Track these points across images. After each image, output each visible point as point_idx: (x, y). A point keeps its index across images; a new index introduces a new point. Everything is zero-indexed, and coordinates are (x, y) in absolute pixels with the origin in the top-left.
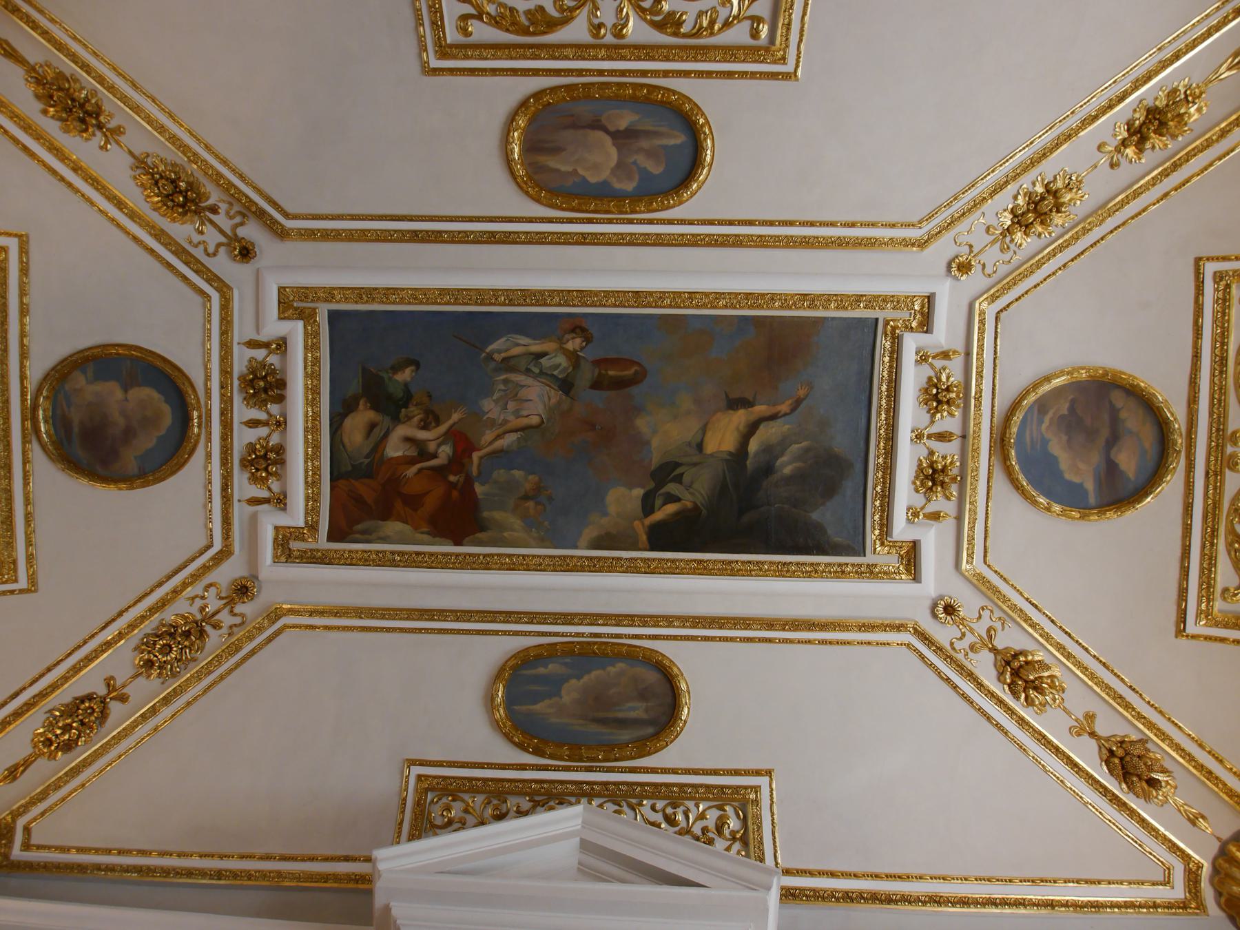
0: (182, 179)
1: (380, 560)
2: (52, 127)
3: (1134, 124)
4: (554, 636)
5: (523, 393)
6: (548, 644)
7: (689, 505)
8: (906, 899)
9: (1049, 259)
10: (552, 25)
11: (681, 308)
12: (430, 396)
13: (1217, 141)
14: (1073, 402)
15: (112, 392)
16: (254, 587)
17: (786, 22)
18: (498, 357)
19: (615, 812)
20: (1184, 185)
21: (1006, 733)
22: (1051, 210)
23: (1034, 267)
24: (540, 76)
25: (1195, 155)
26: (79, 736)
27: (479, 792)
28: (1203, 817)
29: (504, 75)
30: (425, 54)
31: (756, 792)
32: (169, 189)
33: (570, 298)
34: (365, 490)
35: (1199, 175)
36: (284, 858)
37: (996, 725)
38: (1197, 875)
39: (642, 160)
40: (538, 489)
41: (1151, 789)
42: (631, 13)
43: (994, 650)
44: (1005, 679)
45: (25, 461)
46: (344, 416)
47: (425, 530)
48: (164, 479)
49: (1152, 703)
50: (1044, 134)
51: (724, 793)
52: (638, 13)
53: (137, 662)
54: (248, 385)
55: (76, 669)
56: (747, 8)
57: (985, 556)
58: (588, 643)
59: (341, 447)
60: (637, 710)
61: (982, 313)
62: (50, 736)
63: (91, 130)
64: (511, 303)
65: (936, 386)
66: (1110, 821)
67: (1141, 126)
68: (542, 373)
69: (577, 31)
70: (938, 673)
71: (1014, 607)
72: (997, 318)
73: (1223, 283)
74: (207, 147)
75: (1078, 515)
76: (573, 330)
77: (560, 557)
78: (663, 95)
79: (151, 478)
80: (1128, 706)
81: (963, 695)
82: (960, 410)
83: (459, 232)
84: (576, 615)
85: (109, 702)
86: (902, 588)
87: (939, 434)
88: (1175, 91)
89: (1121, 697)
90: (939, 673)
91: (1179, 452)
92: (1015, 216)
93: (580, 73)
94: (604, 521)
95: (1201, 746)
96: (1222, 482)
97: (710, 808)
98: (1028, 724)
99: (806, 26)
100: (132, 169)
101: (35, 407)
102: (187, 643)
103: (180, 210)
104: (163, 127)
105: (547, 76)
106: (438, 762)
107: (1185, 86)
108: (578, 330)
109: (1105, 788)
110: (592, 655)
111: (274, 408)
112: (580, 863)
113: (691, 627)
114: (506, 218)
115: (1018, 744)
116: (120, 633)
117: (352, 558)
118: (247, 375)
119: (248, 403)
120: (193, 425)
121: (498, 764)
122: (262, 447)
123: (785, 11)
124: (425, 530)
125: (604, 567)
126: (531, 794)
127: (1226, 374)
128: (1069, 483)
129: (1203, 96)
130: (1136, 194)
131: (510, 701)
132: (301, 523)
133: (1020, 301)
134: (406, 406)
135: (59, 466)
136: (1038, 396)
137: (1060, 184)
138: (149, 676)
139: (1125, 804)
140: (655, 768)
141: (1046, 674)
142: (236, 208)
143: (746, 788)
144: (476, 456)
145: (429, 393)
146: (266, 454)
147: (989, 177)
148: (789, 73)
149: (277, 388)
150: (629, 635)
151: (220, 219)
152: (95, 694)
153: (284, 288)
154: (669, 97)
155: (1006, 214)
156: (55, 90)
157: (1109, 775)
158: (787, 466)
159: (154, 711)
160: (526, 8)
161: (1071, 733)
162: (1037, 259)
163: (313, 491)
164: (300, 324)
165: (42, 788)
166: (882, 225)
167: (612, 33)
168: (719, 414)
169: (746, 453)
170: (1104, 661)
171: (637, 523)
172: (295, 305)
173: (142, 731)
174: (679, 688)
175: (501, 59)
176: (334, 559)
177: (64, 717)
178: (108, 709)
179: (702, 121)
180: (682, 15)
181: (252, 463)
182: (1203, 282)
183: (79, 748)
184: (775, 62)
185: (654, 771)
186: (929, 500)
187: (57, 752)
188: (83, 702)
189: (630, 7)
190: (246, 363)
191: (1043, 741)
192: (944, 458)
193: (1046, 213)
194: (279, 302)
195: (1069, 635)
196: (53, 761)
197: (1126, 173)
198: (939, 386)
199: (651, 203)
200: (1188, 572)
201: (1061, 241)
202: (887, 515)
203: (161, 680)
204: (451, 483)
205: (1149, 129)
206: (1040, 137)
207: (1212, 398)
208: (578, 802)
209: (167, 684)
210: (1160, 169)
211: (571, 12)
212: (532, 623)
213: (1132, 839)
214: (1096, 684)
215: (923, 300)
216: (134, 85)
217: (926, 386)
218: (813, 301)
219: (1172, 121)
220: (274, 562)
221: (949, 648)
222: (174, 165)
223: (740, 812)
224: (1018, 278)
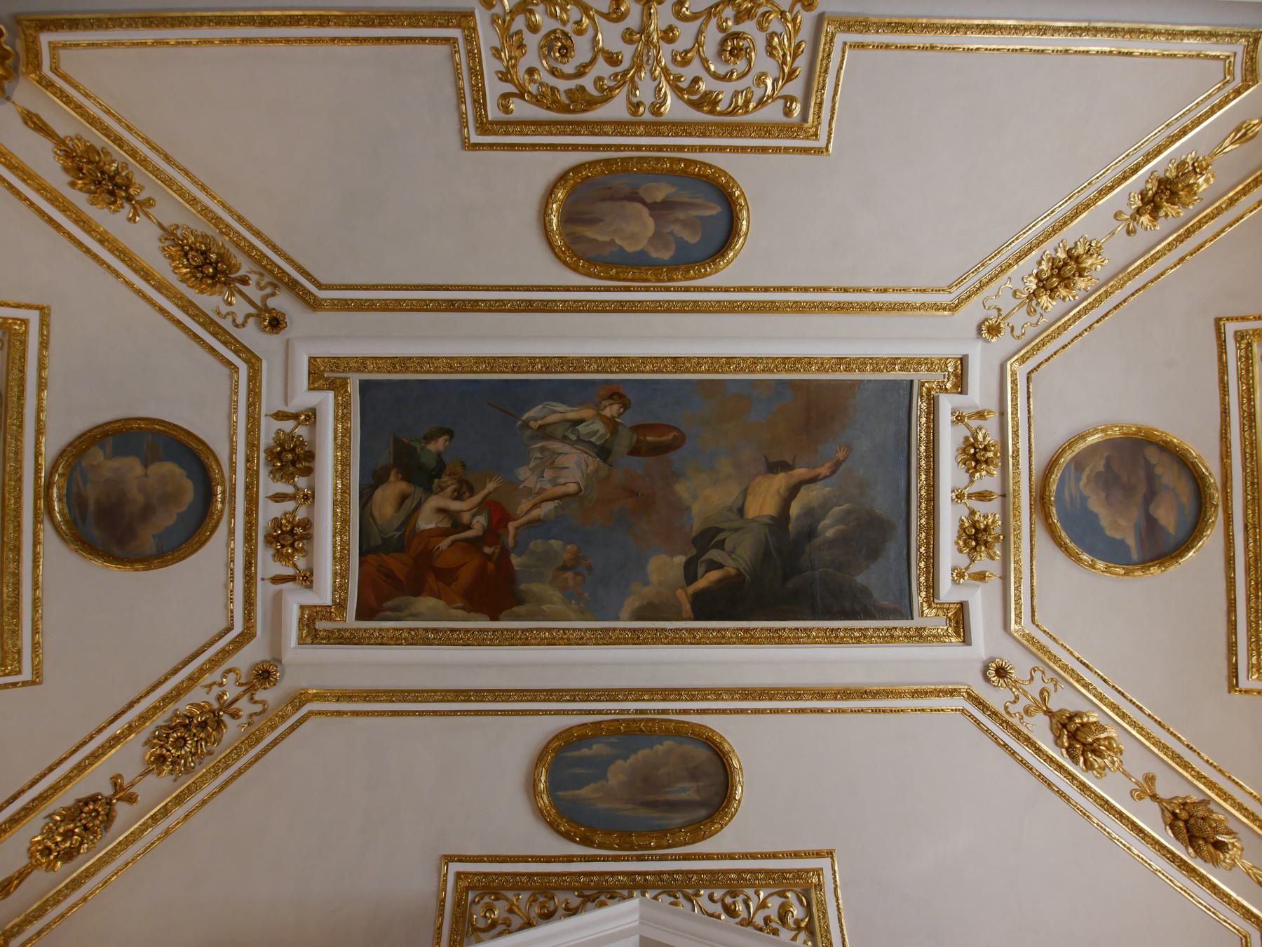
0: (213, 250)
1: (412, 639)
2: (79, 199)
3: (1147, 194)
5: (560, 461)
6: (592, 723)
7: (732, 571)
9: (1075, 321)
10: (591, 103)
11: (720, 373)
12: (464, 466)
13: (1226, 209)
14: (1108, 459)
15: (131, 468)
16: (276, 671)
17: (818, 101)
18: (533, 425)
19: (671, 904)
20: (1198, 250)
21: (1068, 800)
22: (1074, 275)
23: (1061, 329)
24: (578, 150)
25: (1206, 223)
26: (82, 843)
30: (466, 130)
31: (819, 876)
32: (199, 260)
33: (607, 365)
34: (397, 564)
35: (1211, 241)
37: (1058, 792)
39: (678, 230)
41: (1218, 852)
42: (669, 93)
43: (1049, 713)
44: (1063, 743)
45: (36, 543)
46: (374, 488)
47: (460, 605)
48: (184, 558)
49: (1211, 761)
50: (1063, 204)
53: (147, 758)
54: (275, 458)
55: (80, 768)
56: (781, 88)
57: (1033, 616)
58: (634, 720)
60: (687, 791)
61: (1014, 374)
62: (49, 844)
63: (119, 202)
64: (548, 371)
65: (973, 446)
66: (1181, 888)
68: (579, 440)
69: (616, 109)
70: (995, 739)
71: (1065, 667)
73: (1245, 341)
74: (240, 219)
75: (1123, 572)
76: (611, 397)
77: (601, 630)
78: (700, 169)
80: (1186, 766)
81: (1021, 761)
83: (496, 301)
85: (114, 804)
86: (952, 651)
87: (979, 493)
88: (1183, 163)
89: (1179, 757)
90: (996, 739)
91: (1216, 506)
92: (1040, 280)
93: (618, 148)
97: (771, 895)
98: (1089, 789)
99: (837, 105)
100: (160, 240)
101: (49, 486)
102: (202, 735)
103: (210, 281)
104: (195, 199)
105: (586, 150)
106: (478, 857)
107: (1193, 159)
109: (1173, 854)
110: (638, 733)
111: (301, 481)
113: (740, 700)
114: (543, 286)
115: (1081, 811)
116: (130, 726)
117: (383, 637)
119: (274, 477)
120: (217, 501)
121: (543, 857)
122: (288, 522)
123: (817, 91)
125: (648, 638)
126: (580, 890)
127: (1255, 429)
128: (1113, 540)
129: (1210, 168)
130: (1154, 259)
131: (553, 787)
132: (329, 602)
133: (1050, 361)
134: (439, 476)
135: (72, 546)
136: (1074, 454)
137: (1081, 250)
138: (160, 774)
139: (1194, 870)
140: (710, 854)
141: (1102, 736)
142: (268, 279)
143: (807, 871)
144: (512, 526)
145: (463, 462)
146: (292, 529)
147: (1013, 244)
148: (821, 148)
149: (305, 460)
151: (251, 290)
152: (99, 794)
153: (315, 358)
154: (704, 172)
155: (1032, 278)
156: (85, 163)
157: (1174, 839)
158: (829, 529)
159: (165, 812)
160: (567, 87)
161: (1132, 797)
162: (1063, 321)
163: (342, 567)
164: (331, 394)
165: (39, 903)
166: (914, 290)
168: (759, 479)
169: (788, 517)
170: (1159, 719)
171: (679, 592)
172: (326, 375)
173: (151, 834)
174: (731, 765)
175: (541, 135)
176: (363, 638)
177: (66, 822)
178: (115, 811)
179: (737, 193)
180: (718, 95)
181: (277, 539)
183: (80, 856)
184: (807, 138)
185: (708, 857)
186: (973, 560)
187: (56, 863)
188: (86, 804)
189: (668, 87)
191: (1106, 806)
193: (1069, 278)
194: (310, 373)
195: (1123, 694)
196: (52, 873)
198: (976, 446)
200: (1236, 626)
201: (1085, 304)
202: (933, 577)
203: (173, 777)
204: (485, 554)
205: (1161, 199)
206: (1060, 206)
207: (1244, 452)
208: (631, 897)
210: (1175, 236)
211: (611, 91)
212: (574, 701)
213: (1205, 907)
214: (1153, 744)
215: (956, 362)
216: (167, 158)
217: (963, 446)
218: (850, 364)
219: (1182, 191)
221: (1003, 713)
222: (205, 236)
223: (804, 899)
224: (1047, 340)
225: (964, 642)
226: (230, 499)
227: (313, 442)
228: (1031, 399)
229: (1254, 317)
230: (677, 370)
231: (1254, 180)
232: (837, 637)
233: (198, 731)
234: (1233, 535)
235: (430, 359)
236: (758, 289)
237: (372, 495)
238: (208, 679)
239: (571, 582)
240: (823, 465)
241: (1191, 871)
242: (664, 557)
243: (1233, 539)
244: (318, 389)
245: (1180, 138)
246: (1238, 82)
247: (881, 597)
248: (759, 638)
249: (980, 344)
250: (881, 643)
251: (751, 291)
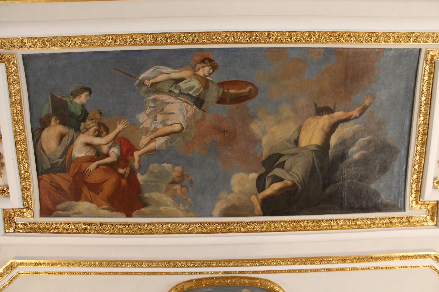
5: (168, 108)
7: (289, 183)
11: (283, 43)
12: (100, 113)
18: (148, 83)
40: (182, 176)
46: (42, 130)
47: (106, 207)
58: (223, 278)
59: (42, 152)
64: (156, 43)
68: (181, 93)
76: (203, 61)
77: (201, 223)
94: (230, 196)
108: (206, 61)
124: (106, 207)
134: (84, 120)
144: (136, 154)
145: (99, 111)
150: (250, 271)
168: (310, 119)
169: (328, 146)
171: (253, 198)
202: (421, 184)
212: (184, 267)
218: (378, 37)
225: (436, 225)
232: (356, 225)
237: (40, 135)
239: (179, 192)
240: (354, 110)
247: (384, 197)
248: (306, 227)
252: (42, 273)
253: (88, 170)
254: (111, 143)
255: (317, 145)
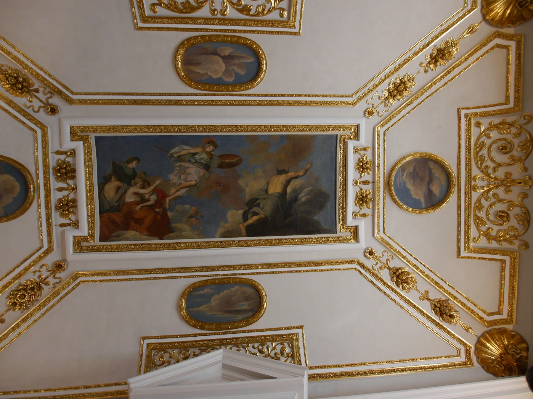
0: (20, 76)
3: (433, 55)
4: (206, 276)
5: (188, 171)
6: (204, 280)
7: (263, 216)
8: (359, 373)
9: (403, 110)
10: (194, 9)
11: (256, 132)
12: (145, 174)
13: (464, 62)
14: (414, 167)
16: (65, 265)
18: (175, 155)
19: (237, 350)
20: (452, 79)
21: (395, 302)
22: (403, 90)
23: (397, 113)
25: (456, 68)
27: (176, 348)
28: (471, 328)
29: (173, 31)
30: (136, 21)
31: (297, 336)
32: (14, 81)
34: (117, 217)
35: (457, 75)
36: (86, 387)
37: (391, 299)
38: (470, 351)
39: (235, 68)
41: (451, 319)
42: (228, 5)
43: (389, 268)
44: (394, 280)
46: (105, 184)
48: (18, 217)
50: (399, 59)
51: (283, 338)
52: (231, 5)
53: (8, 304)
54: (57, 172)
56: (278, 4)
57: (384, 230)
58: (222, 278)
59: (104, 198)
60: (244, 306)
61: (378, 132)
64: (180, 132)
65: (362, 162)
66: (436, 333)
67: (435, 56)
69: (204, 12)
70: (368, 279)
71: (396, 250)
72: (384, 133)
73: (468, 118)
74: (32, 62)
75: (418, 212)
76: (209, 143)
77: (207, 242)
79: (11, 217)
80: (441, 287)
81: (378, 287)
82: (372, 171)
83: (155, 100)
84: (216, 266)
86: (352, 246)
87: (364, 181)
88: (447, 42)
89: (438, 283)
91: (455, 185)
92: (389, 92)
93: (207, 30)
94: (227, 225)
95: (468, 300)
96: (471, 196)
97: (278, 344)
98: (403, 297)
99: (303, 13)
102: (33, 293)
103: (20, 91)
104: (9, 52)
105: (192, 31)
106: (156, 337)
107: (451, 40)
108: (211, 143)
109: (434, 320)
111: (70, 182)
112: (223, 374)
113: (266, 268)
114: (176, 94)
115: (400, 306)
117: (112, 248)
118: (56, 167)
119: (58, 180)
120: (31, 191)
121: (184, 335)
122: (65, 200)
123: (294, 6)
125: (227, 245)
128: (415, 199)
129: (458, 44)
130: (435, 83)
131: (188, 307)
132: (86, 234)
136: (401, 165)
137: (406, 79)
138: (14, 310)
139: (441, 326)
141: (409, 276)
142: (48, 90)
143: (292, 334)
144: (167, 199)
145: (144, 172)
146: (67, 203)
148: (296, 32)
149: (72, 173)
150: (240, 274)
151: (40, 95)
153: (73, 126)
157: (435, 315)
158: (303, 197)
159: (18, 326)
162: (398, 109)
164: (82, 143)
167: (220, 13)
168: (274, 177)
169: (286, 193)
170: (431, 269)
171: (241, 225)
172: (79, 134)
173: (12, 335)
174: (262, 295)
175: (171, 23)
179: (261, 52)
180: (250, 6)
181: (61, 208)
182: (461, 118)
184: (290, 28)
185: (253, 331)
186: (361, 209)
189: (228, 2)
190: (56, 162)
192: (366, 191)
193: (401, 91)
194: (71, 133)
195: (417, 260)
197: (431, 74)
199: (241, 87)
201: (407, 102)
202: (345, 216)
203: (21, 311)
205: (438, 57)
206: (397, 60)
207: (466, 163)
208: (221, 348)
209: (24, 312)
210: (443, 73)
212: (196, 272)
213: (445, 340)
214: (428, 279)
215: (355, 127)
218: (311, 128)
220: (74, 253)
221: (371, 269)
222: (16, 70)
223: (290, 345)
226: (37, 190)
227: (74, 164)
228: (385, 142)
229: (472, 108)
230: (237, 130)
231: (475, 50)
232: (306, 242)
233: (30, 291)
234: (461, 197)
235: (126, 127)
236: (271, 95)
238: (33, 269)
239: (194, 223)
241: (440, 326)
242: (234, 211)
243: (461, 198)
244: (76, 140)
245: (446, 31)
246: (469, 7)
247: (325, 226)
249: (365, 119)
250: (324, 243)
251: (268, 96)
252: (97, 281)
253: (135, 210)
254: (151, 193)
255: (279, 193)
